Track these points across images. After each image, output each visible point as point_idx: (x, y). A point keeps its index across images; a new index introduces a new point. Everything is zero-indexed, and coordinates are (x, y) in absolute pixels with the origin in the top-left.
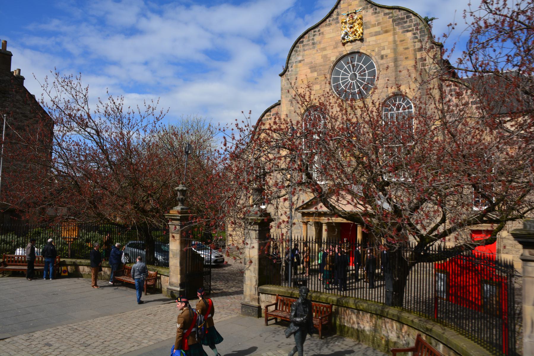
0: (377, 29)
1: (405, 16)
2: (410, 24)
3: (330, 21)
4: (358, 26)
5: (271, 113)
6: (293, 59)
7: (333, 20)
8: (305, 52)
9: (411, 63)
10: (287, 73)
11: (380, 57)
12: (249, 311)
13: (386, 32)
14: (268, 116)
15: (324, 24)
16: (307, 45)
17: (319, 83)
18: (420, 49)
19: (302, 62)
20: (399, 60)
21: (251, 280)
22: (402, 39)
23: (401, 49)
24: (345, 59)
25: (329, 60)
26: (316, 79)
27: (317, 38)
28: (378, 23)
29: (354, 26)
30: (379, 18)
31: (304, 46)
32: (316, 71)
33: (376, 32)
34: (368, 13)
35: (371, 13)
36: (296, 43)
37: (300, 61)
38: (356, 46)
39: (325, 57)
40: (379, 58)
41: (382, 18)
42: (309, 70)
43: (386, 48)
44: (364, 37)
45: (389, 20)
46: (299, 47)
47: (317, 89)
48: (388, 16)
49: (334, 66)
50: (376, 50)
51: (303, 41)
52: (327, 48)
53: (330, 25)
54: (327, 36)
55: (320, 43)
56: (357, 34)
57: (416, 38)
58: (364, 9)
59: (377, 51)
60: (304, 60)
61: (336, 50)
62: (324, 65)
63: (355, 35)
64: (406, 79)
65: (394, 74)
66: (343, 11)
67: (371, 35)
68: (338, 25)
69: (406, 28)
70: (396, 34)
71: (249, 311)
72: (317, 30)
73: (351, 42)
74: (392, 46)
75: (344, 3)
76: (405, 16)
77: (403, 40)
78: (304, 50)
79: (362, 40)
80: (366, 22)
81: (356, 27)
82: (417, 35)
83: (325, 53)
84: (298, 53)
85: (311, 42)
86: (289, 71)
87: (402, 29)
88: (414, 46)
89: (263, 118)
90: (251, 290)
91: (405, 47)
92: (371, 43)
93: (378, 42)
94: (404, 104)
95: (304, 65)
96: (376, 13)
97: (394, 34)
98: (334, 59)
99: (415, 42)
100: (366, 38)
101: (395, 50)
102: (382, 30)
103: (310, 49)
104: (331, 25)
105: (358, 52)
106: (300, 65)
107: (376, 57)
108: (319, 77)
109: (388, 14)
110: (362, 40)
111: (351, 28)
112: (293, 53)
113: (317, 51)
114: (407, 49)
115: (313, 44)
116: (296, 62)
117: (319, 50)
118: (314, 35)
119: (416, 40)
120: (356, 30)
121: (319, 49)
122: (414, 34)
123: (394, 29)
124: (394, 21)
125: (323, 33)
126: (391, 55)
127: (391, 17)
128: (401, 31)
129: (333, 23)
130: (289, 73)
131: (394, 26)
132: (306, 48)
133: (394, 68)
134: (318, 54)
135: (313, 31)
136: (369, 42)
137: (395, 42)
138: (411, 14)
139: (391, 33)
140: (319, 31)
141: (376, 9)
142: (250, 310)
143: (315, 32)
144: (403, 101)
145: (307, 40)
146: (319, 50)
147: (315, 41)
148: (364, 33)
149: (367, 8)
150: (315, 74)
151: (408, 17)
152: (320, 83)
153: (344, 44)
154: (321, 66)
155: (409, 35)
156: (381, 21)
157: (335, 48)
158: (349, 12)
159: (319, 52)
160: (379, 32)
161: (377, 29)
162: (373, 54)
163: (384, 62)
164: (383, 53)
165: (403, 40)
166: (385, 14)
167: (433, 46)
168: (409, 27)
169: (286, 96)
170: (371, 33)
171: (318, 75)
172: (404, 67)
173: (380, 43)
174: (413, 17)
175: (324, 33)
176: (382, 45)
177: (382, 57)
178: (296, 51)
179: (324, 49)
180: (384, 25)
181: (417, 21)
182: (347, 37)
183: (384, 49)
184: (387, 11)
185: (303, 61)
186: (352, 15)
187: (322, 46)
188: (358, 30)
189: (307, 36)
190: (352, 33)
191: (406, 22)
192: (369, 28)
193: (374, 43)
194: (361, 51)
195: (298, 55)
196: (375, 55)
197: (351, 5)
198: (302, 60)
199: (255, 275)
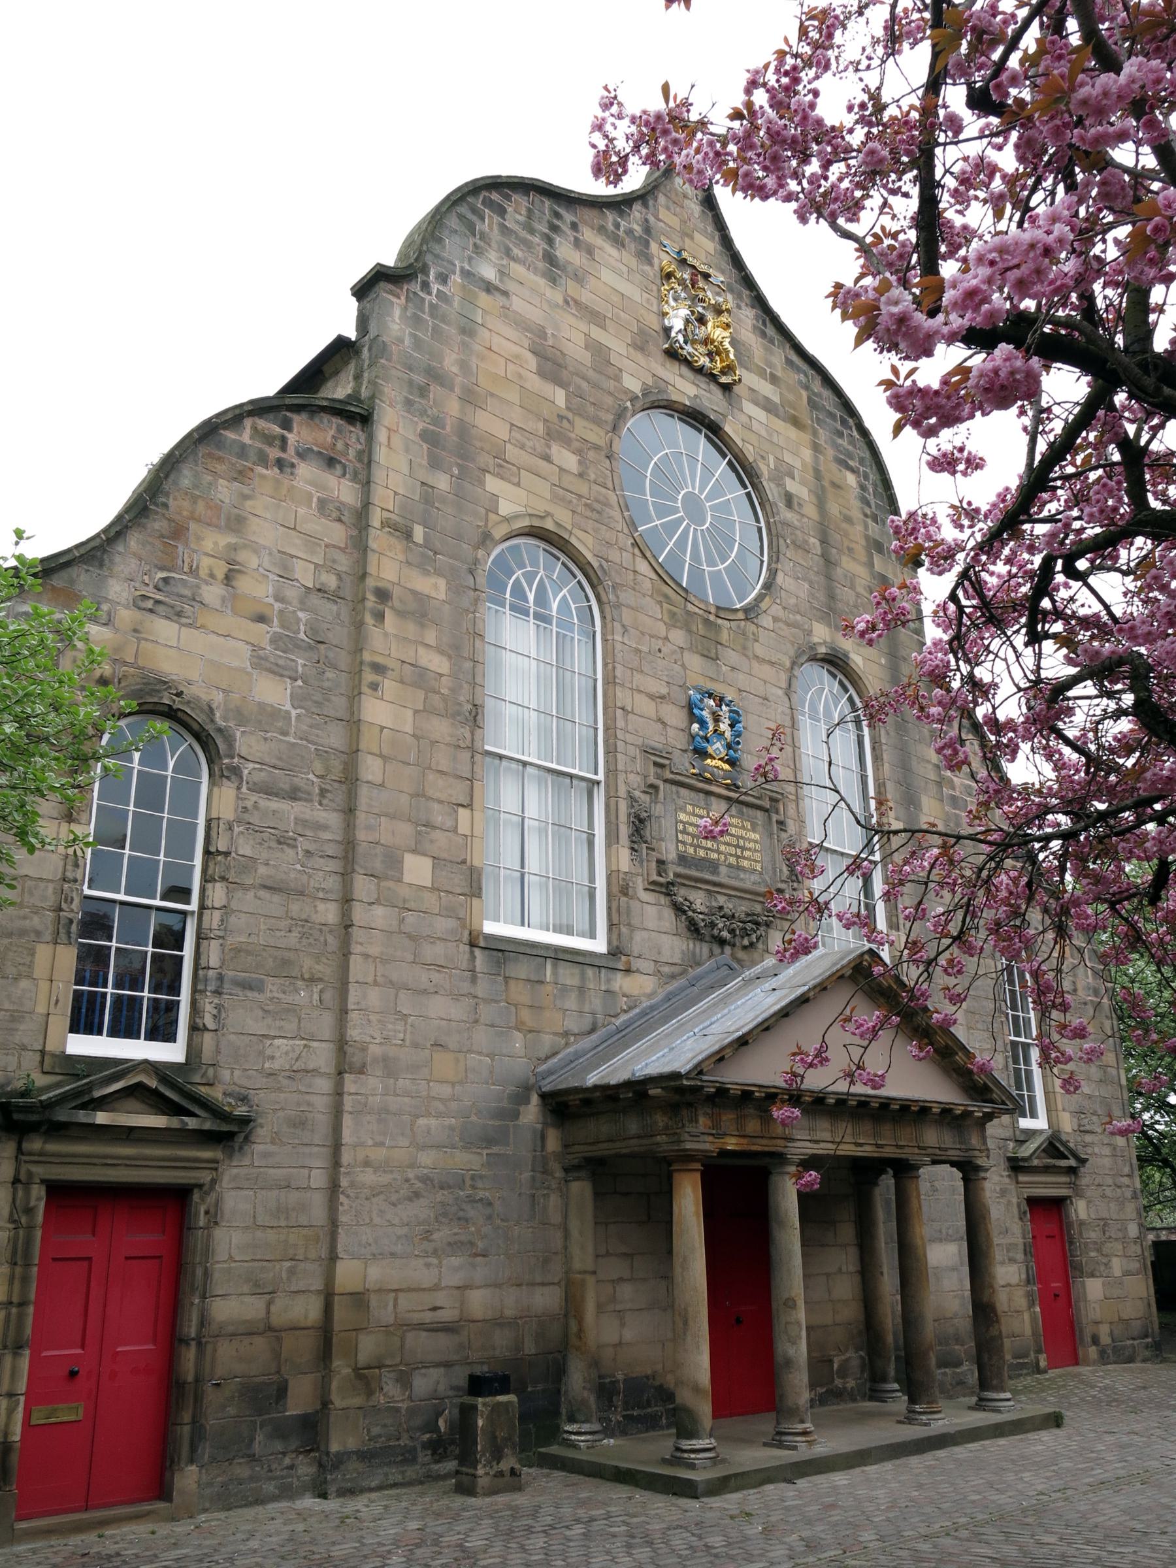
14: (269, 439)
17: (576, 445)
19: (501, 300)
23: (834, 508)
25: (618, 379)
37: (489, 288)
42: (532, 362)
53: (618, 242)
55: (579, 278)
59: (772, 466)
60: (505, 294)
72: (568, 217)
83: (596, 333)
98: (633, 384)
104: (624, 246)
106: (484, 299)
109: (798, 370)
113: (566, 302)
118: (554, 228)
132: (516, 251)
140: (574, 226)
150: (560, 397)
164: (792, 486)
168: (850, 456)
171: (568, 408)
193: (763, 433)
194: (728, 429)
198: (497, 289)
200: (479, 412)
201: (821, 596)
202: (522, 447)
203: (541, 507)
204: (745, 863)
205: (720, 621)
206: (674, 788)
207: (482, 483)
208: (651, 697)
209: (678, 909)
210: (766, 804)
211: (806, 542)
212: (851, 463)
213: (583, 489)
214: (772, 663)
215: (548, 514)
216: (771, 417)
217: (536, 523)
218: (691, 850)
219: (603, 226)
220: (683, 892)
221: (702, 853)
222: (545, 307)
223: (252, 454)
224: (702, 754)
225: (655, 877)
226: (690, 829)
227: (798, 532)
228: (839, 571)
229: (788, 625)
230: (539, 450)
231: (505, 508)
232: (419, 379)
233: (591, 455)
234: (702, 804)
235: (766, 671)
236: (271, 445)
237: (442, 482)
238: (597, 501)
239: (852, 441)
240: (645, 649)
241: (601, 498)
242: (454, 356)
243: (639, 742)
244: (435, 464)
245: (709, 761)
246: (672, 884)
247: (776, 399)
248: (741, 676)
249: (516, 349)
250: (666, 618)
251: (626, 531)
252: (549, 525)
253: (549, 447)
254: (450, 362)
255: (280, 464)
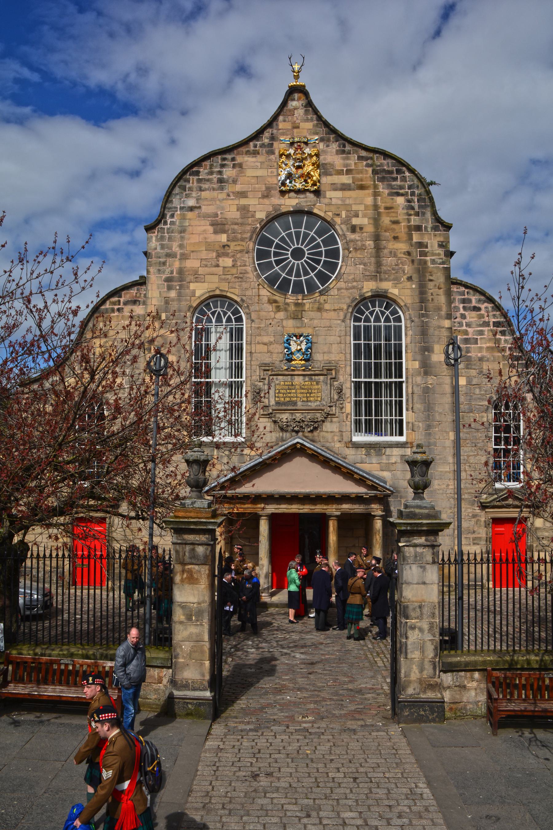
0: (346, 179)
1: (395, 168)
2: (402, 183)
3: (255, 146)
4: (311, 167)
5: (122, 300)
6: (176, 202)
7: (263, 146)
8: (203, 193)
9: (402, 247)
10: (161, 225)
11: (350, 229)
12: (422, 713)
13: (362, 187)
14: (114, 303)
15: (243, 149)
16: (208, 180)
17: (232, 254)
18: (418, 228)
19: (196, 212)
20: (382, 238)
21: (422, 650)
22: (388, 205)
23: (386, 220)
24: (282, 220)
25: (253, 216)
26: (224, 246)
27: (229, 173)
28: (347, 170)
29: (304, 165)
30: (349, 162)
31: (200, 181)
32: (224, 231)
33: (343, 184)
34: (329, 149)
35: (334, 150)
36: (184, 172)
37: (191, 209)
38: (306, 202)
39: (244, 209)
40: (348, 229)
41: (355, 164)
42: (211, 229)
43: (360, 215)
44: (322, 188)
45: (367, 169)
46: (189, 182)
47: (226, 265)
48: (365, 163)
49: (262, 228)
50: (344, 214)
51: (197, 173)
52: (250, 195)
53: (255, 153)
54: (250, 173)
55: (235, 182)
56: (309, 181)
57: (413, 208)
58: (322, 140)
59: (344, 216)
60: (200, 207)
61: (266, 201)
62: (242, 224)
63: (306, 181)
64: (393, 272)
65: (373, 260)
66: (283, 134)
67: (335, 187)
68: (272, 157)
69: (395, 189)
70: (379, 195)
71: (422, 713)
72: (229, 156)
73: (298, 192)
74: (370, 212)
75: (284, 121)
76: (395, 168)
77: (391, 208)
78: (201, 189)
79: (317, 193)
80: (326, 164)
81: (308, 168)
82: (413, 204)
83: (243, 202)
84: (187, 192)
85: (215, 177)
86: (165, 223)
87: (388, 188)
88: (409, 221)
89: (103, 307)
90: (422, 670)
91: (393, 219)
92: (334, 201)
93: (347, 202)
94: (387, 313)
95: (199, 217)
96: (343, 152)
97: (376, 194)
98: (261, 215)
99: (410, 215)
100: (325, 191)
101: (376, 221)
102: (353, 183)
103: (214, 189)
104: (258, 153)
105: (310, 213)
106: (190, 215)
107: (343, 226)
108: (232, 244)
109: (366, 159)
110: (317, 193)
111: (299, 167)
112: (177, 190)
113: (229, 195)
114: (396, 222)
115: (221, 181)
116: (182, 208)
117: (231, 194)
118: (223, 166)
119: (412, 212)
120: (309, 173)
121: (233, 193)
122: (409, 201)
123: (376, 187)
124: (375, 172)
125: (240, 165)
126: (370, 229)
127: (371, 166)
128: (386, 192)
129: (264, 150)
130: (166, 227)
131: (375, 181)
133: (374, 251)
134: (230, 202)
135: (220, 157)
136: (331, 199)
137: (376, 207)
138: (404, 168)
139: (370, 191)
140: (233, 159)
141: (344, 146)
142: (425, 711)
143: (224, 159)
144: (387, 308)
145: (206, 171)
146: (231, 194)
147: (225, 176)
148: (321, 181)
149: (329, 140)
150: (223, 238)
151: (399, 172)
152: (233, 256)
153: (283, 193)
154: (236, 224)
155: (400, 200)
156: (353, 167)
157: (266, 196)
158: (296, 140)
159: (232, 197)
160: (349, 185)
161: (346, 179)
162: (338, 220)
163: (357, 238)
164: (355, 221)
165: (391, 208)
166: (360, 158)
167: (438, 226)
168: (401, 187)
169: (159, 270)
170: (334, 184)
171: (228, 241)
172: (391, 252)
173: (350, 205)
174: (407, 174)
175: (244, 167)
176: (354, 208)
177: (353, 229)
178: (184, 188)
179: (243, 194)
180: (359, 176)
181: (413, 181)
182: (290, 182)
183: (357, 216)
184: (363, 153)
185: (199, 210)
186: (299, 146)
187: (238, 188)
188: (312, 173)
189: (207, 163)
190: (299, 177)
191: (395, 179)
192: (331, 175)
193: (340, 202)
194: (316, 211)
195: (187, 196)
196: (342, 224)
197: (298, 127)
198: (196, 207)
199: (432, 638)
200: (188, 261)
201: (372, 268)
202: (206, 266)
203: (213, 286)
204: (312, 399)
205: (305, 301)
206: (275, 377)
207: (188, 287)
208: (265, 344)
209: (275, 422)
210: (325, 372)
211: (364, 245)
212: (401, 191)
213: (234, 271)
214: (334, 310)
215: (217, 288)
216: (344, 192)
217: (211, 294)
218: (283, 399)
219: (248, 151)
220: (278, 415)
221: (288, 399)
222: (218, 202)
223: (109, 311)
224: (290, 360)
225: (262, 413)
226: (282, 391)
227: (359, 243)
228: (386, 251)
229: (347, 289)
230: (214, 264)
231: (198, 294)
232: (162, 260)
233: (239, 255)
234: (290, 380)
235: (332, 314)
236: (115, 305)
237: (173, 294)
238: (241, 273)
239: (404, 179)
240: (263, 325)
241: (243, 271)
242: (177, 244)
243: (259, 363)
244: (170, 288)
245: (293, 362)
246: (271, 413)
247: (350, 181)
248: (316, 321)
249: (203, 228)
250: (274, 310)
251: (255, 280)
252: (218, 292)
253: (218, 261)
254: (175, 248)
255: (119, 310)
